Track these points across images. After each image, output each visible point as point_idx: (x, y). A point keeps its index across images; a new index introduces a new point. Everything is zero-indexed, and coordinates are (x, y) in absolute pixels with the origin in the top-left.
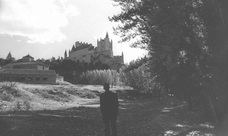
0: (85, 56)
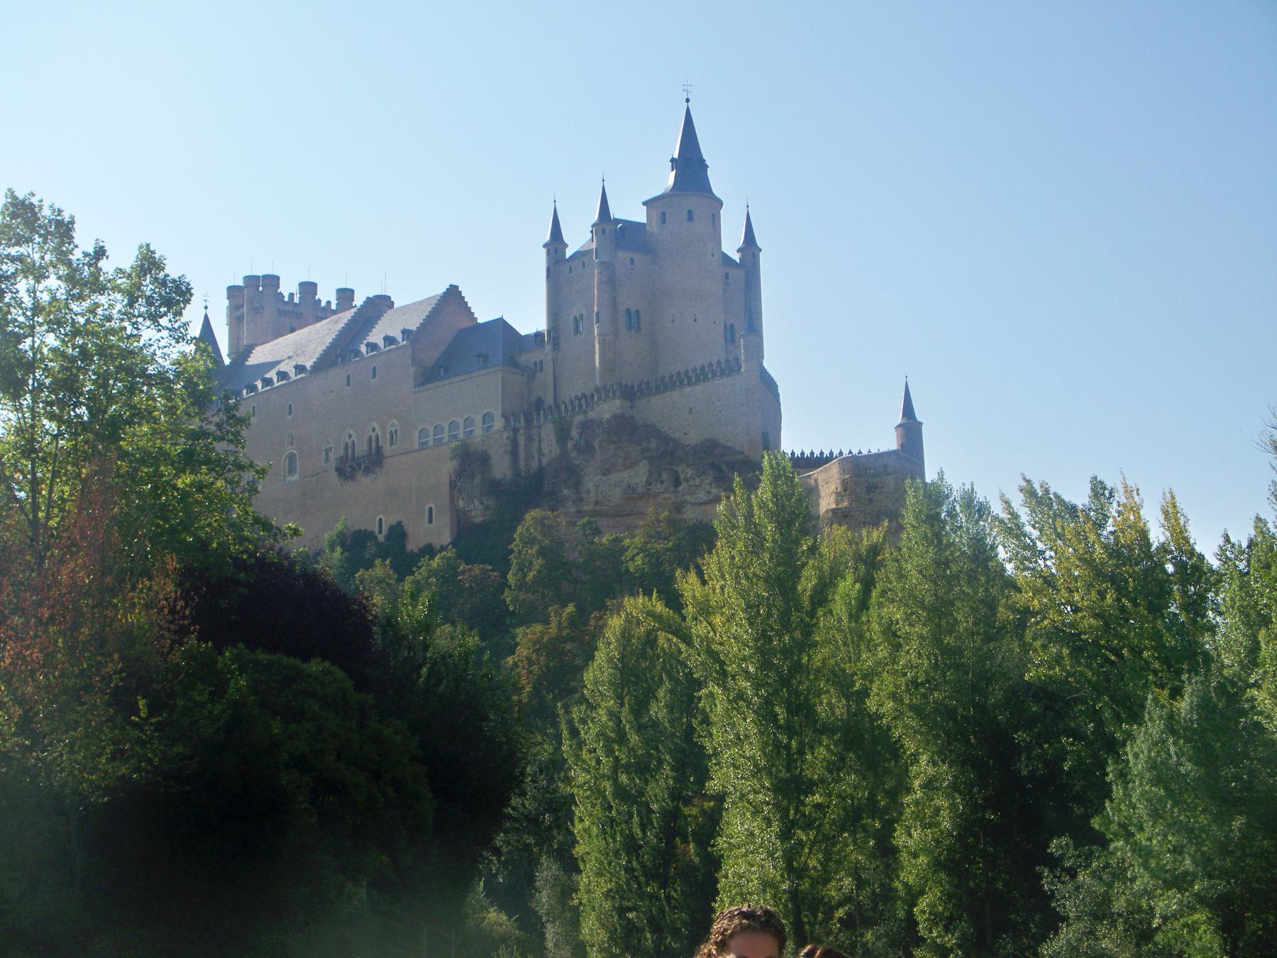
0: (374, 460)
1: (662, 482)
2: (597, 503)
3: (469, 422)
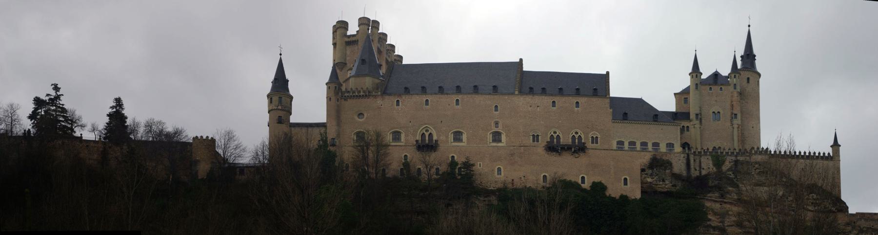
0: (578, 148)
3: (656, 145)
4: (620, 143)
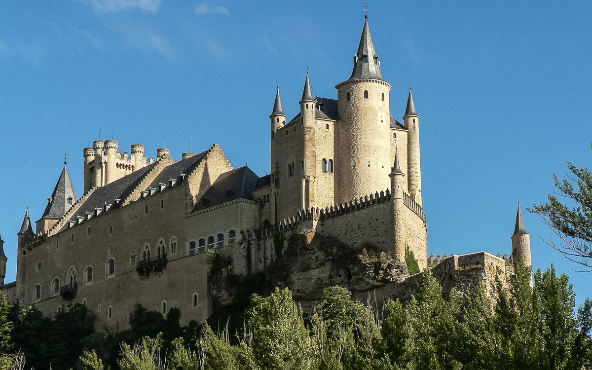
1: (340, 276)
2: (298, 291)
3: (221, 237)
4: (192, 245)
